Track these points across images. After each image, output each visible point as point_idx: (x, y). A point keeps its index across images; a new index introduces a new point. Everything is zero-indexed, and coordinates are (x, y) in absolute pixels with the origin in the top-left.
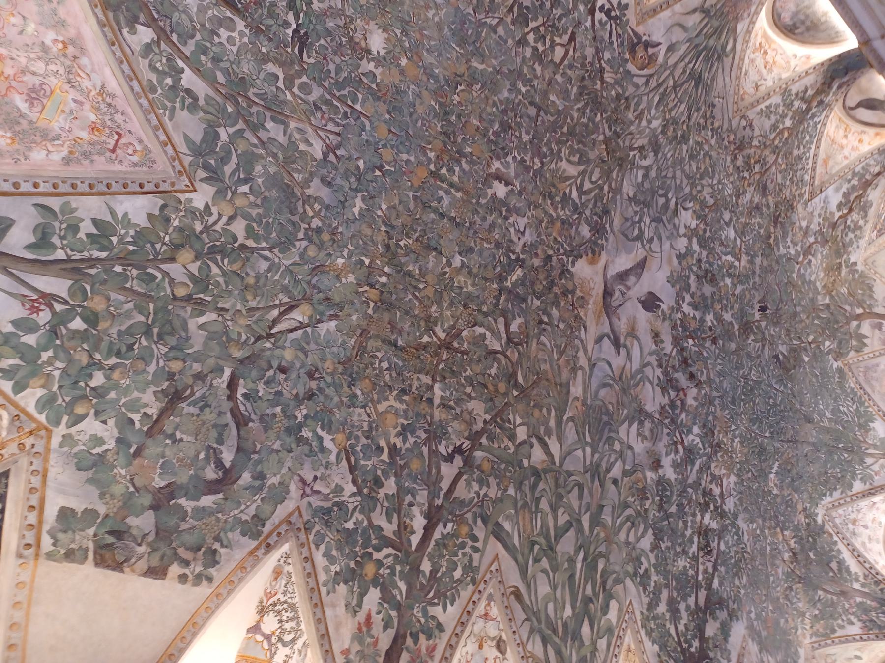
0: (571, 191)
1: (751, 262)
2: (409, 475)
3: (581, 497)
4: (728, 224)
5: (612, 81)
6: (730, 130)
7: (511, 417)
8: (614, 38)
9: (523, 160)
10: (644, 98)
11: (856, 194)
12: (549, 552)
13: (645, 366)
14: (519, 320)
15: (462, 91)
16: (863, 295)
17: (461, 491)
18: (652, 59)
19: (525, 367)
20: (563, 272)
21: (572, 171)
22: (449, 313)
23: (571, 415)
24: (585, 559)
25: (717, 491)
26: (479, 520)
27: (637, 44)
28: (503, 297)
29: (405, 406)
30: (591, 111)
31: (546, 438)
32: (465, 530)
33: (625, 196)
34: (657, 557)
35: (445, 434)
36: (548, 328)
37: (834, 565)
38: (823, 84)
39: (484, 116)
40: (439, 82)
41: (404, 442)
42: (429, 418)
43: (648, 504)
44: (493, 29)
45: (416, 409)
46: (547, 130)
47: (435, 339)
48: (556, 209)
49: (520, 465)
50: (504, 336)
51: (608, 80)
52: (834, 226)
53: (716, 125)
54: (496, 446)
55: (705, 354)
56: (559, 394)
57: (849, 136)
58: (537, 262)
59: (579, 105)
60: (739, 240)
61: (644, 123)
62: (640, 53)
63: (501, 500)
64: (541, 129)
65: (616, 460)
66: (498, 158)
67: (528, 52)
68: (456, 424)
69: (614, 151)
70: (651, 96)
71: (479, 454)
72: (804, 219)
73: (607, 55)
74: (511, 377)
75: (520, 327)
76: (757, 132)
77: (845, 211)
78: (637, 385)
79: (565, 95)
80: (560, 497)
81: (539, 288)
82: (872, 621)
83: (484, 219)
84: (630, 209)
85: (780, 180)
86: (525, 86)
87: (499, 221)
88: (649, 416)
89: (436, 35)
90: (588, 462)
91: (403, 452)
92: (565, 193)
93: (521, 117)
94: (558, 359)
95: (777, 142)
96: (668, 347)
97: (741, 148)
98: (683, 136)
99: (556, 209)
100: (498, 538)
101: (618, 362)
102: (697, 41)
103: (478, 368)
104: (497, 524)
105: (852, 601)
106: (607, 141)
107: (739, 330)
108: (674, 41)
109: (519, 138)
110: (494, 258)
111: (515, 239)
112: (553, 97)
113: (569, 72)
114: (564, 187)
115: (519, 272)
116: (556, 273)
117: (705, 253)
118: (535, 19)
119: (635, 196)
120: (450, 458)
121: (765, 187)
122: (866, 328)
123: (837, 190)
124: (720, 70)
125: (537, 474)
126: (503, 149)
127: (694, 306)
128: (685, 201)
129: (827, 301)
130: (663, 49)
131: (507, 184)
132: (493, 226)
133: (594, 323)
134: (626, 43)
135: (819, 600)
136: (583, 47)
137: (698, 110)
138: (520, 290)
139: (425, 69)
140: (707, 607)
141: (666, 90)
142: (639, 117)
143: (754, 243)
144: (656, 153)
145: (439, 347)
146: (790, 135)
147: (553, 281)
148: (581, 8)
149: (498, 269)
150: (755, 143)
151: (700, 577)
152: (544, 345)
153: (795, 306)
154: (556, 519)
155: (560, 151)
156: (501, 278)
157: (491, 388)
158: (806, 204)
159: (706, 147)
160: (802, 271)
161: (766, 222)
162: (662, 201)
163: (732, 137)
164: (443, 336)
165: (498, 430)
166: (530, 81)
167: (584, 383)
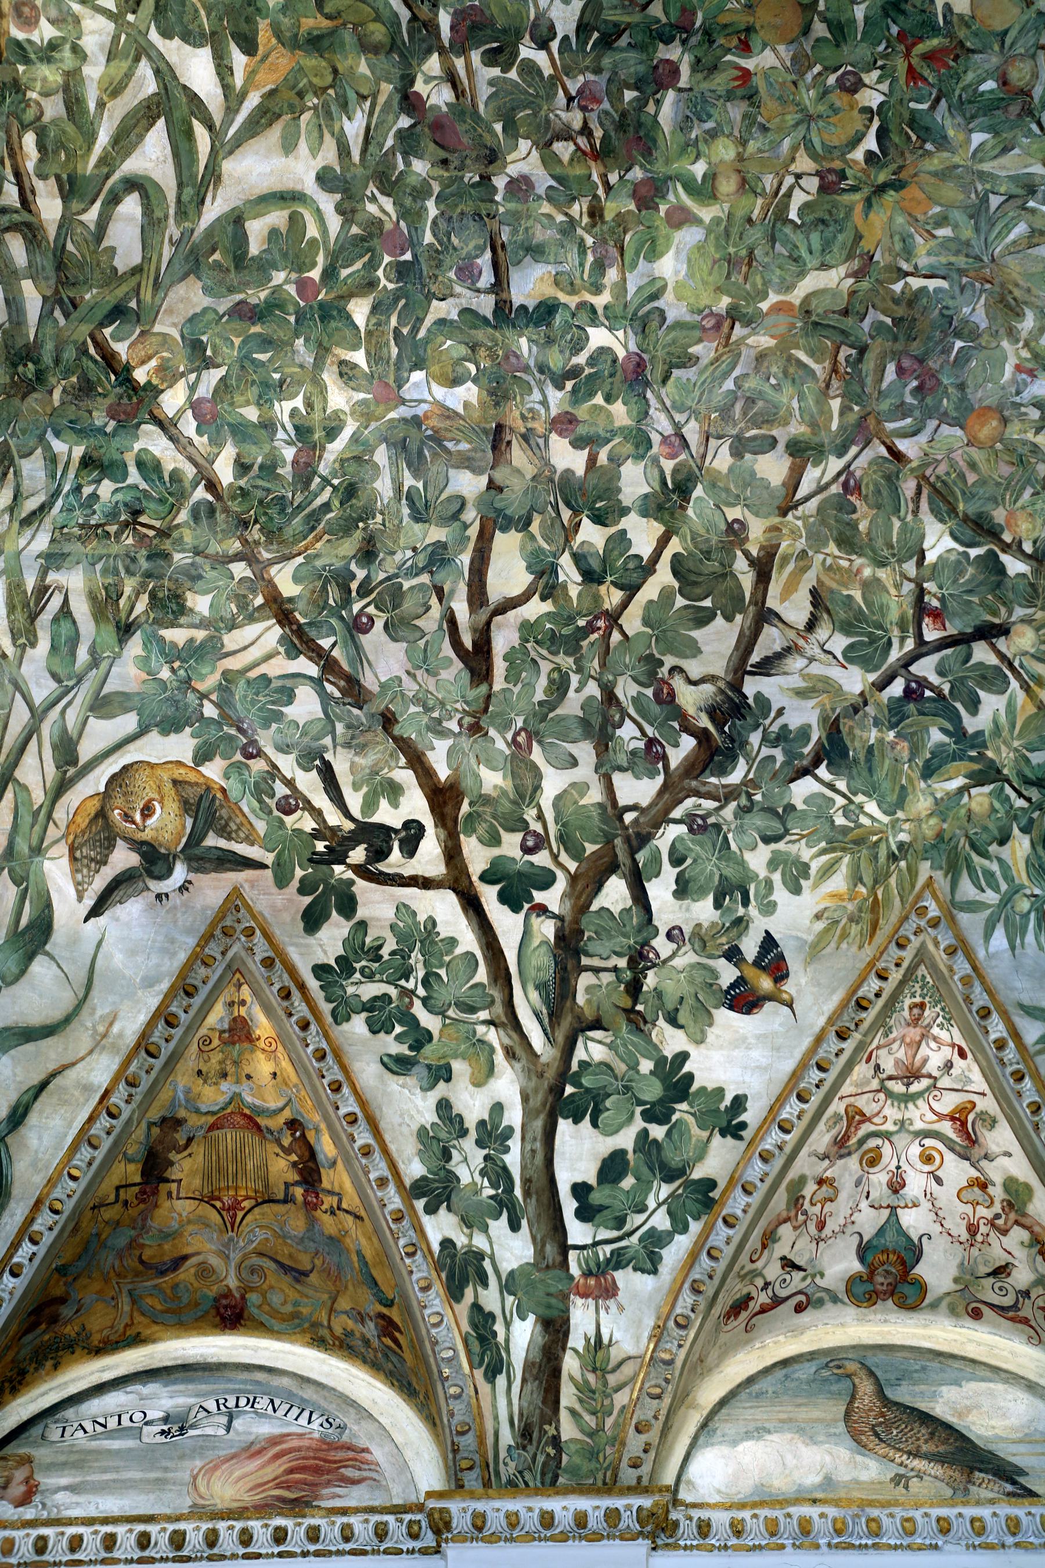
0: (223, 70)
5: (231, 640)
8: (309, 783)
9: (501, 55)
10: (42, 690)
15: (857, 140)
21: (253, 168)
27: (195, 839)
30: (269, 469)
39: (736, 111)
40: (959, 107)
44: (802, 453)
46: (437, 256)
51: (249, 632)
59: (336, 447)
62: (166, 823)
64: (467, 241)
67: (634, 482)
69: (86, 389)
73: (305, 706)
79: (418, 443)
86: (603, 351)
89: (1014, 267)
92: (249, 46)
106: (137, 403)
108: (40, 967)
109: (546, 137)
112: (465, 396)
113: (437, 534)
126: (607, 42)
136: (424, 662)
139: (1028, 111)
148: (493, 780)
155: (347, 212)
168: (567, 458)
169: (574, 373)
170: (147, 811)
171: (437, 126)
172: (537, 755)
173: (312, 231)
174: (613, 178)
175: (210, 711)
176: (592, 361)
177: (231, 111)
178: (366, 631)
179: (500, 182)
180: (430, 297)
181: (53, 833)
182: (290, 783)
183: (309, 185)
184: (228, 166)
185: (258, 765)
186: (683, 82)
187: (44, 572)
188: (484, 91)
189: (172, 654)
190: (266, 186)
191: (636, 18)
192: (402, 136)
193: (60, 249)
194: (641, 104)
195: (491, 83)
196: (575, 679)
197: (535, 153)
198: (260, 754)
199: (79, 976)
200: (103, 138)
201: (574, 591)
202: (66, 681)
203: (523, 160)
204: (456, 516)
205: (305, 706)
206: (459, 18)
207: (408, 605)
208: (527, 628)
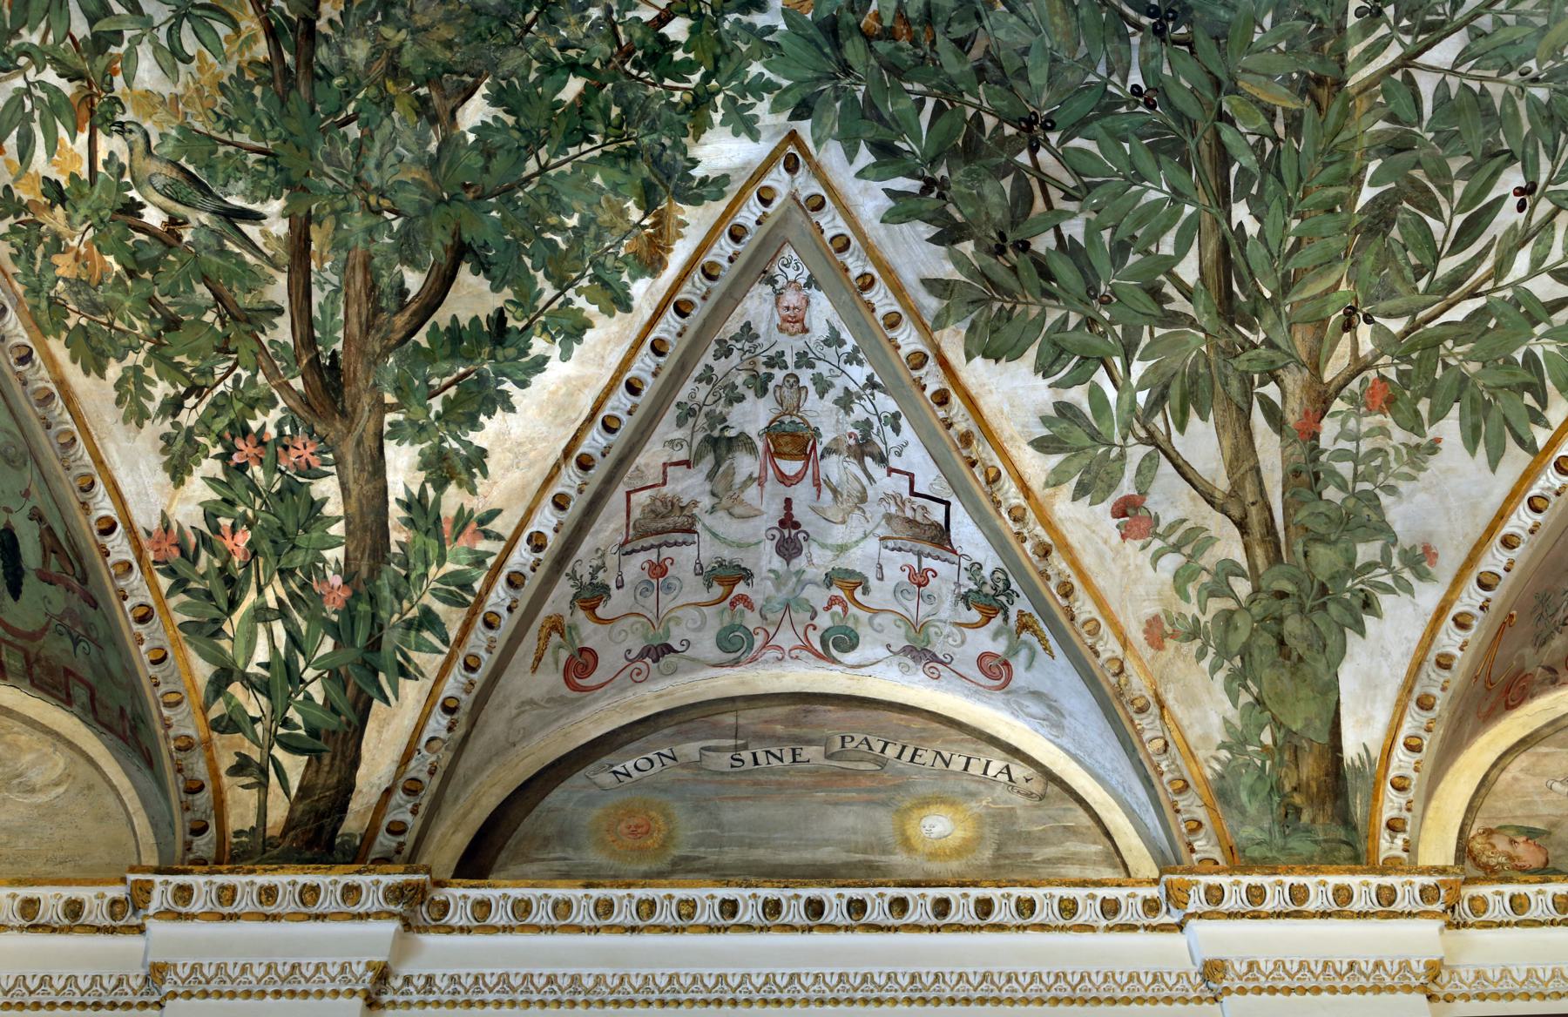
37: (472, 297)
82: (233, 585)
105: (303, 450)
135: (233, 216)
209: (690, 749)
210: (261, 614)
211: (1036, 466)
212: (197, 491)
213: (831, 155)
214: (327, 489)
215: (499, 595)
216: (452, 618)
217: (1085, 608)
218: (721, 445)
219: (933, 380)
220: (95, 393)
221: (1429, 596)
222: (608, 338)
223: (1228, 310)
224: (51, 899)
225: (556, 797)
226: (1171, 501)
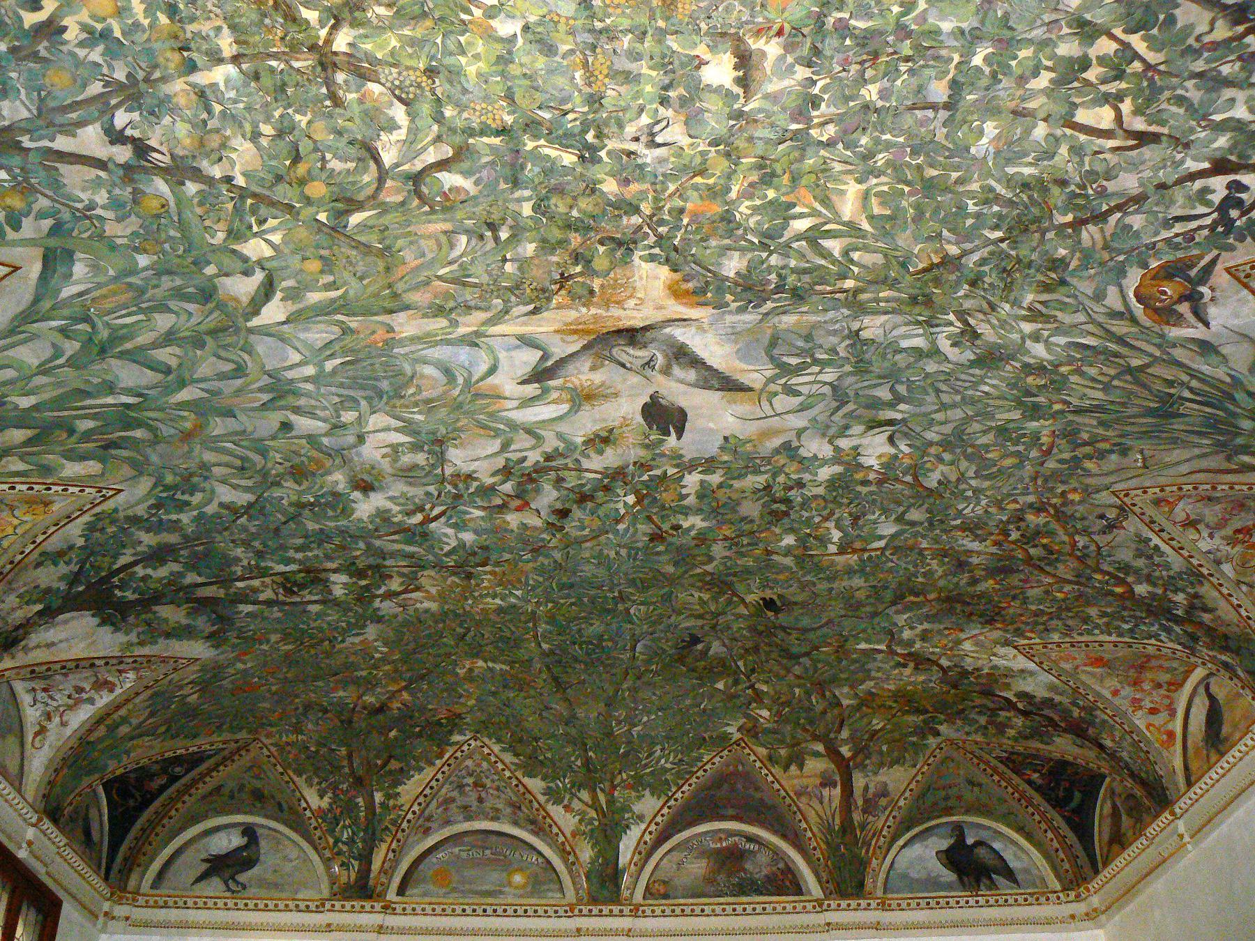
0: (801, 216)
1: (850, 572)
2: (32, 77)
3: (222, 376)
4: (900, 519)
6: (1088, 492)
7: (272, 222)
8: (1179, 228)
9: (815, 102)
10: (1081, 317)
11: (1056, 718)
12: (96, 350)
13: (529, 431)
14: (467, 184)
16: (881, 753)
17: (73, 176)
18: (1167, 315)
19: (387, 219)
20: (620, 244)
21: (848, 208)
22: (394, 43)
23: (353, 325)
24: (128, 406)
25: (395, 585)
26: (47, 223)
27: (1189, 279)
28: (496, 141)
29: (146, 22)
30: (1000, 217)
31: (279, 295)
32: (16, 202)
33: (855, 326)
34: (218, 516)
35: (152, 113)
36: (490, 244)
37: (394, 765)
38: (1226, 637)
41: (81, 44)
42: (157, 75)
43: (289, 484)
45: (157, 46)
46: (910, 136)
47: (323, 33)
48: (747, 195)
49: (199, 264)
50: (419, 166)
51: (1084, 235)
52: (987, 693)
53: (1089, 465)
54: (199, 211)
55: (621, 527)
56: (376, 295)
57: (1162, 692)
58: (610, 187)
59: (1000, 189)
60: (882, 544)
61: (1027, 327)
63: (114, 248)
65: (324, 421)
66: (789, 48)
67: (1068, 48)
68: (182, 129)
69: (937, 282)
70: (1090, 327)
71: (161, 186)
72: (976, 644)
73: (1137, 221)
74: (346, 203)
75: (457, 190)
76: (1101, 540)
77: (1020, 706)
78: (485, 427)
79: (1008, 151)
80: (199, 343)
81: (559, 205)
83: (635, 56)
84: (834, 340)
85: (1031, 593)
86: (986, 59)
87: (648, 88)
88: (442, 459)
90: (290, 375)
91: (64, 48)
93: (911, 71)
94: (439, 278)
95: (1098, 577)
96: (596, 463)
97: (1060, 516)
98: (1036, 407)
99: (747, 195)
100: (49, 261)
101: (507, 383)
102: (1239, 396)
103: (322, 134)
104: (69, 256)
105: (353, 793)
106: (948, 262)
107: (706, 573)
108: (1225, 350)
110: (564, 101)
111: (630, 130)
113: (1064, 150)
114: (805, 201)
115: (569, 159)
116: (607, 226)
117: (820, 491)
118: (1154, 44)
119: (866, 342)
120: (116, 137)
121: (1007, 571)
122: (817, 766)
123: (1052, 688)
124: (1197, 451)
125: (207, 294)
126: (816, 51)
127: (704, 492)
128: (906, 435)
129: (845, 702)
130: (1198, 332)
131: (743, 82)
132: (629, 78)
133: (556, 327)
134: (1180, 254)
136: (1134, 166)
137: (1102, 423)
138: (531, 170)
140: (198, 600)
141: (1116, 355)
142: (1034, 315)
143: (890, 571)
144: (979, 362)
145: (313, 48)
146: (1121, 596)
147: (589, 228)
148: (1222, 141)
149: (546, 115)
150: (1081, 541)
151: (240, 584)
152: (452, 246)
153: (807, 654)
154: (155, 345)
155: (878, 173)
156: (532, 126)
157: (301, 169)
158: (1007, 643)
159: (1034, 453)
160: (879, 657)
161: (942, 583)
162: (884, 393)
163: (1076, 497)
164: (341, 42)
165: (230, 206)
166: (1007, 71)
167: (428, 335)
168: (1043, 80)
169: (994, 75)
170: (1165, 293)
171: (845, 132)
172: (1218, 118)
173: (885, 188)
174: (891, 50)
175: (1121, 258)
176: (990, 65)
177: (819, 214)
178: (1105, 189)
179: (880, 104)
180: (932, 141)
181: (1157, 329)
182: (1177, 235)
183: (863, 187)
184: (846, 219)
185: (1159, 245)
186: (847, 16)
187: (1021, 307)
188: (833, 110)
189: (1084, 266)
190: (858, 204)
191: (809, 40)
192: (846, 147)
193: (870, 282)
194: (854, 36)
195: (828, 106)
196: (1179, 92)
197: (870, 87)
198: (1154, 244)
199: (1237, 338)
200: (823, 262)
201: (1124, 85)
202: (1079, 308)
203: (871, 93)
204: (1057, 140)
205: (1137, 221)
206: (794, 120)
207: (1100, 168)
208: (1137, 112)
209: (456, 850)
210: (345, 827)
211: (542, 799)
212: (326, 799)
213: (486, 740)
214: (360, 801)
215: (405, 825)
216: (393, 829)
217: (555, 830)
218: (461, 787)
219: (514, 782)
220: (300, 781)
221: (643, 826)
222: (429, 772)
223: (589, 771)
224: (302, 905)
225: (421, 867)
226: (576, 805)
